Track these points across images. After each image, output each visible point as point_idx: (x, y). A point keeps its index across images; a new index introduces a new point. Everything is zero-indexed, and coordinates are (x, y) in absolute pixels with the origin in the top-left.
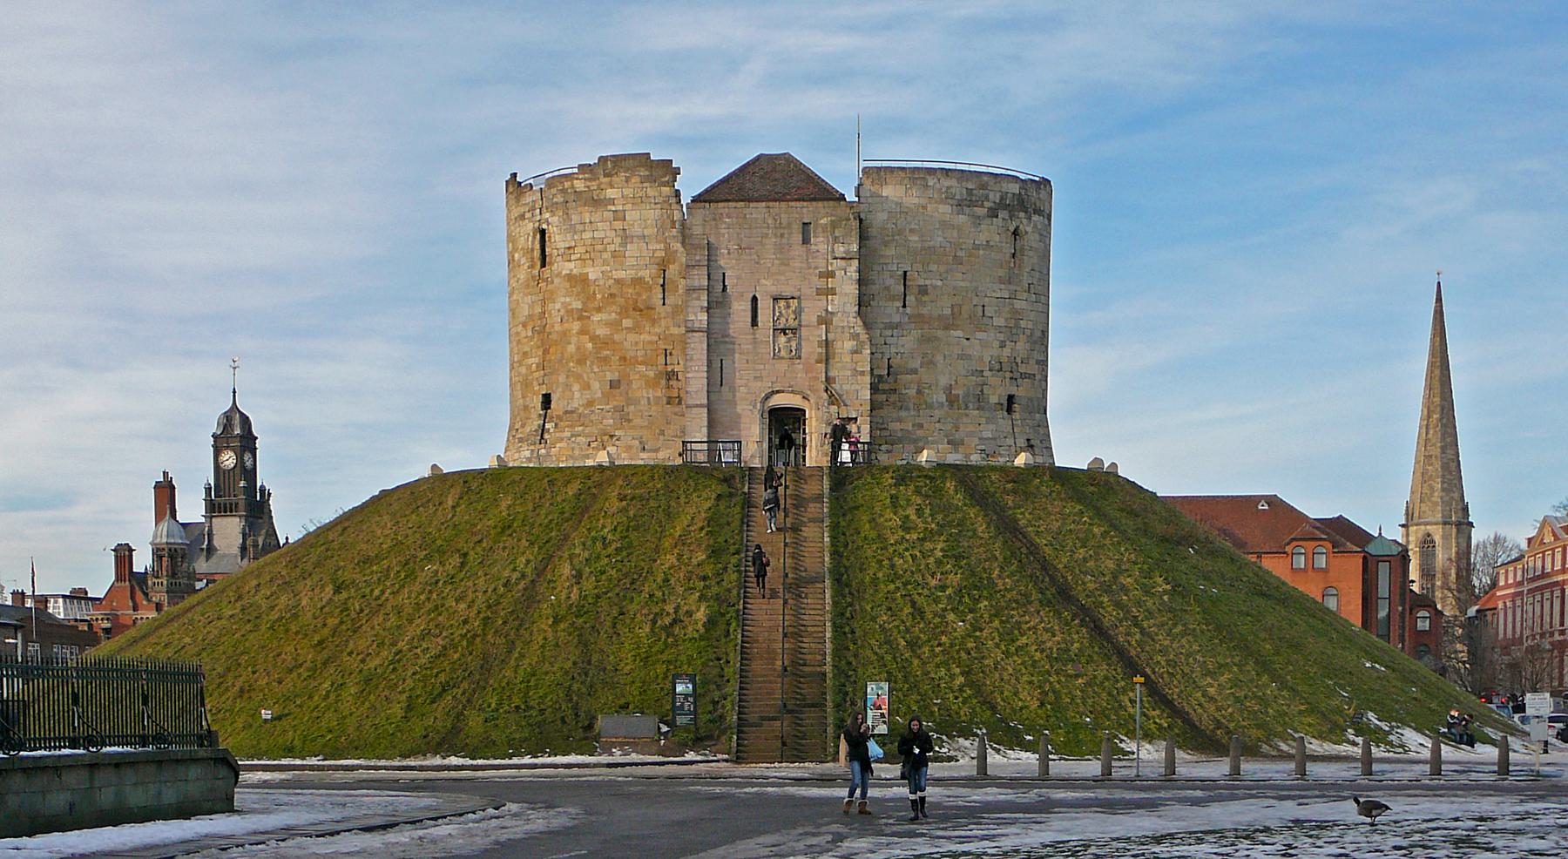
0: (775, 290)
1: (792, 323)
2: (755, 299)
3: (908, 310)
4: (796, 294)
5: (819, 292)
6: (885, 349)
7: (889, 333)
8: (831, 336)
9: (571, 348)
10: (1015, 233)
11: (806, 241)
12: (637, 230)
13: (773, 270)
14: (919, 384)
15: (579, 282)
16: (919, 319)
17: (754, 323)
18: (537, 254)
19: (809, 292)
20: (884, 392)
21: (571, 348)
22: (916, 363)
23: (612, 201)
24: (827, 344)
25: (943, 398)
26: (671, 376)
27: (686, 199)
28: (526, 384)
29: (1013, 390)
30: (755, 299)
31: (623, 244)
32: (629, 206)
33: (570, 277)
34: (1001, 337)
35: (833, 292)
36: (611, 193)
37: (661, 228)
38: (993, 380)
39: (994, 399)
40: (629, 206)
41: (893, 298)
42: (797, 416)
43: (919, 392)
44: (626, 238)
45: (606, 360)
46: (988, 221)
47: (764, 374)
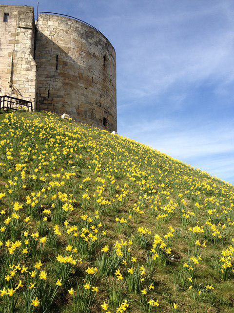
3: (58, 71)
5: (10, 42)
6: (48, 86)
8: (15, 62)
11: (5, 20)
16: (63, 75)
20: (46, 104)
22: (62, 93)
25: (75, 110)
29: (106, 117)
34: (101, 93)
35: (17, 42)
38: (98, 109)
39: (98, 117)
41: (52, 65)
43: (63, 106)
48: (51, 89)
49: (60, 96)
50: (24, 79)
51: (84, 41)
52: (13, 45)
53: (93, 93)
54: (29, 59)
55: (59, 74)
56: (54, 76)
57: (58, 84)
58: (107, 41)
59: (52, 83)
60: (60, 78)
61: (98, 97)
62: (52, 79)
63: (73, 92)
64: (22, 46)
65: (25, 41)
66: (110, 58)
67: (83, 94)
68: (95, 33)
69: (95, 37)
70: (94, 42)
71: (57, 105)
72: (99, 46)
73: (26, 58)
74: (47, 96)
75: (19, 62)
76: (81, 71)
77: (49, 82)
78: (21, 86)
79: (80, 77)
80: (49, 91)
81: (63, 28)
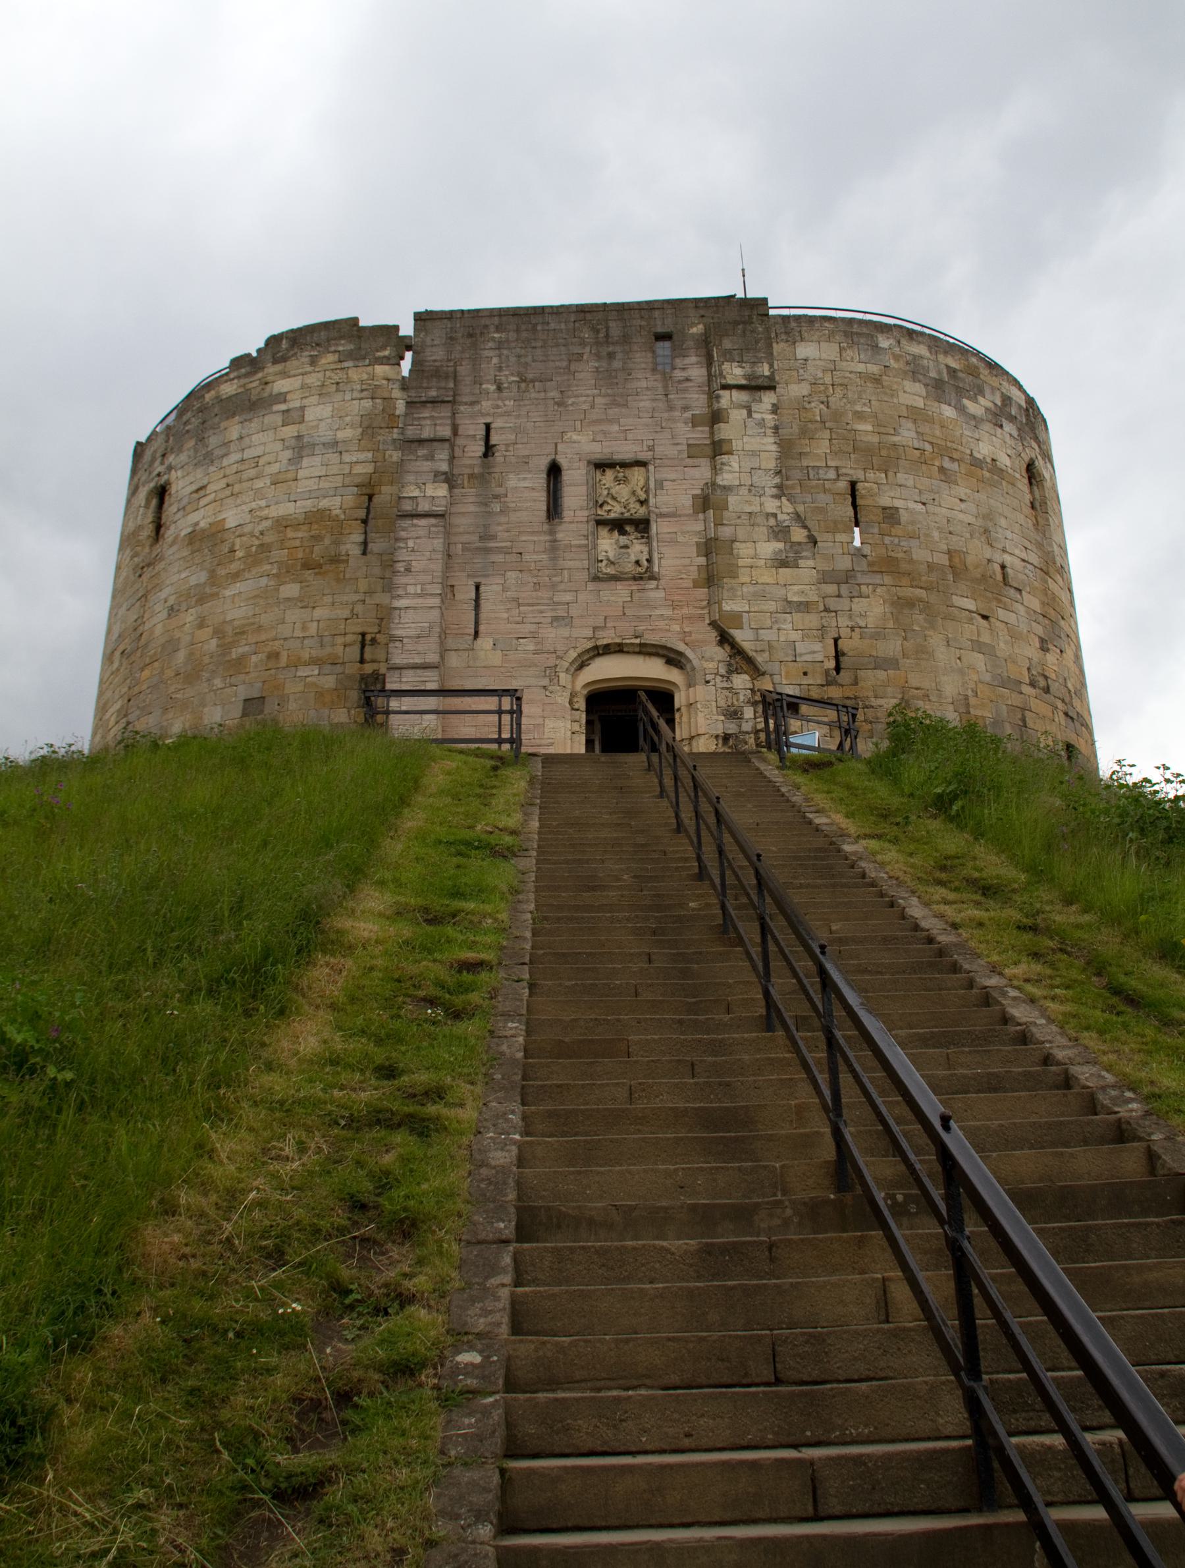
0: (599, 450)
1: (641, 512)
2: (554, 471)
4: (642, 456)
5: (693, 451)
7: (831, 589)
8: (726, 532)
9: (181, 656)
12: (324, 433)
13: (595, 417)
14: (904, 689)
16: (888, 565)
17: (554, 510)
18: (148, 530)
19: (672, 451)
21: (181, 656)
22: (892, 647)
23: (282, 398)
24: (709, 547)
30: (554, 471)
31: (296, 460)
32: (314, 399)
33: (195, 538)
34: (1039, 630)
36: (281, 385)
37: (369, 429)
40: (314, 399)
42: (663, 699)
44: (301, 448)
45: (241, 661)
46: (987, 427)
47: (574, 611)
48: (845, 632)
49: (885, 660)
50: (772, 606)
51: (948, 412)
52: (705, 463)
53: (1014, 635)
54: (781, 517)
55: (870, 564)
56: (847, 577)
57: (872, 609)
58: (1031, 401)
59: (844, 604)
60: (877, 579)
61: (1031, 651)
62: (844, 589)
63: (936, 641)
64: (748, 464)
65: (752, 443)
67: (978, 646)
68: (984, 372)
69: (987, 391)
70: (987, 409)
71: (880, 702)
72: (1009, 427)
73: (768, 515)
74: (831, 664)
75: (741, 533)
76: (956, 543)
77: (832, 603)
78: (766, 635)
79: (957, 567)
80: (836, 641)
81: (861, 368)
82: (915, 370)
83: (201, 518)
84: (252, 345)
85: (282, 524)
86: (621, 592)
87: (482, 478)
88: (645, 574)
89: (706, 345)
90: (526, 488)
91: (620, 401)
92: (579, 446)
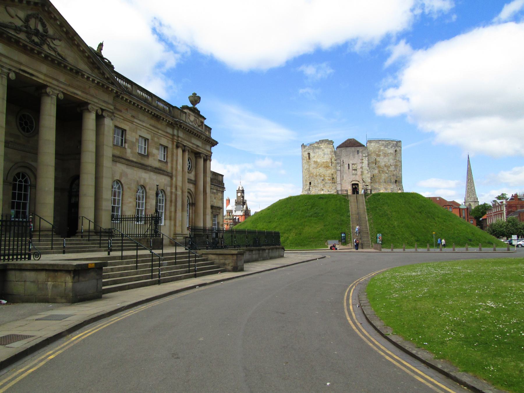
0: (352, 163)
10: (396, 151)
12: (326, 153)
15: (315, 162)
17: (349, 168)
24: (362, 172)
26: (333, 178)
27: (335, 147)
28: (306, 181)
33: (314, 162)
36: (321, 146)
37: (331, 152)
66: (398, 150)
82: (383, 145)
83: (314, 159)
84: (318, 141)
85: (323, 162)
86: (354, 176)
87: (343, 165)
88: (356, 175)
89: (362, 152)
90: (347, 166)
91: (354, 158)
92: (351, 162)
